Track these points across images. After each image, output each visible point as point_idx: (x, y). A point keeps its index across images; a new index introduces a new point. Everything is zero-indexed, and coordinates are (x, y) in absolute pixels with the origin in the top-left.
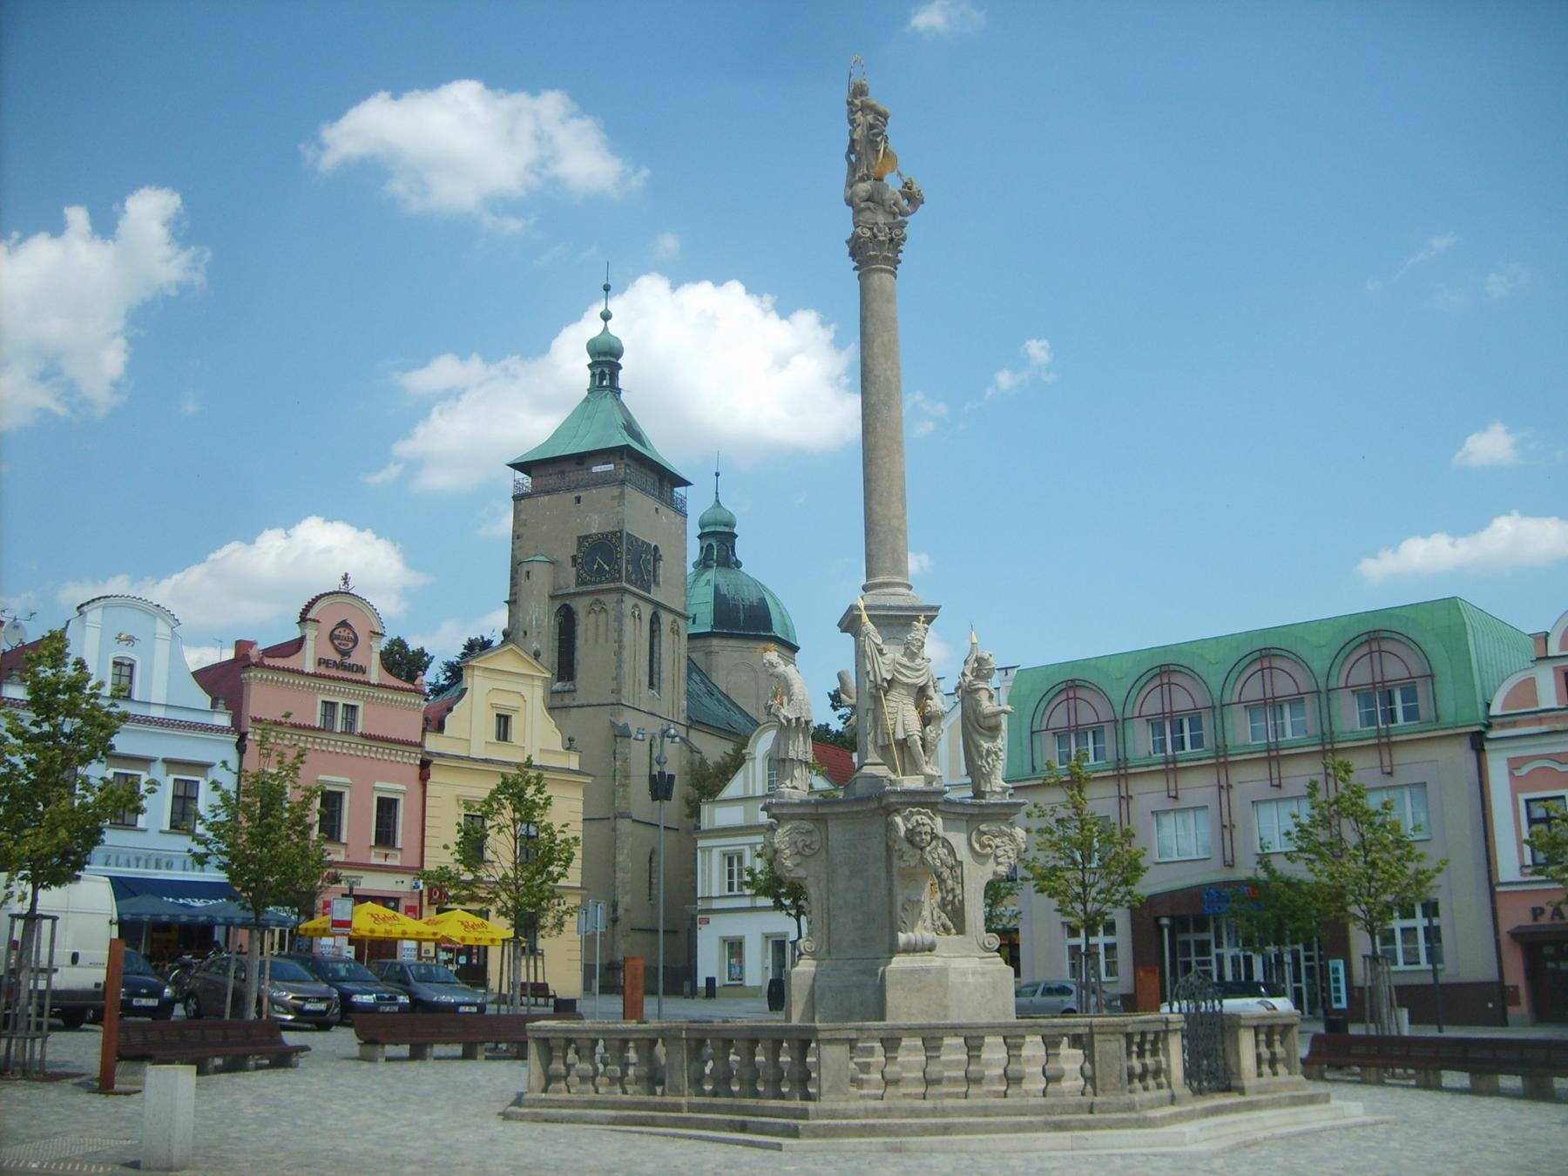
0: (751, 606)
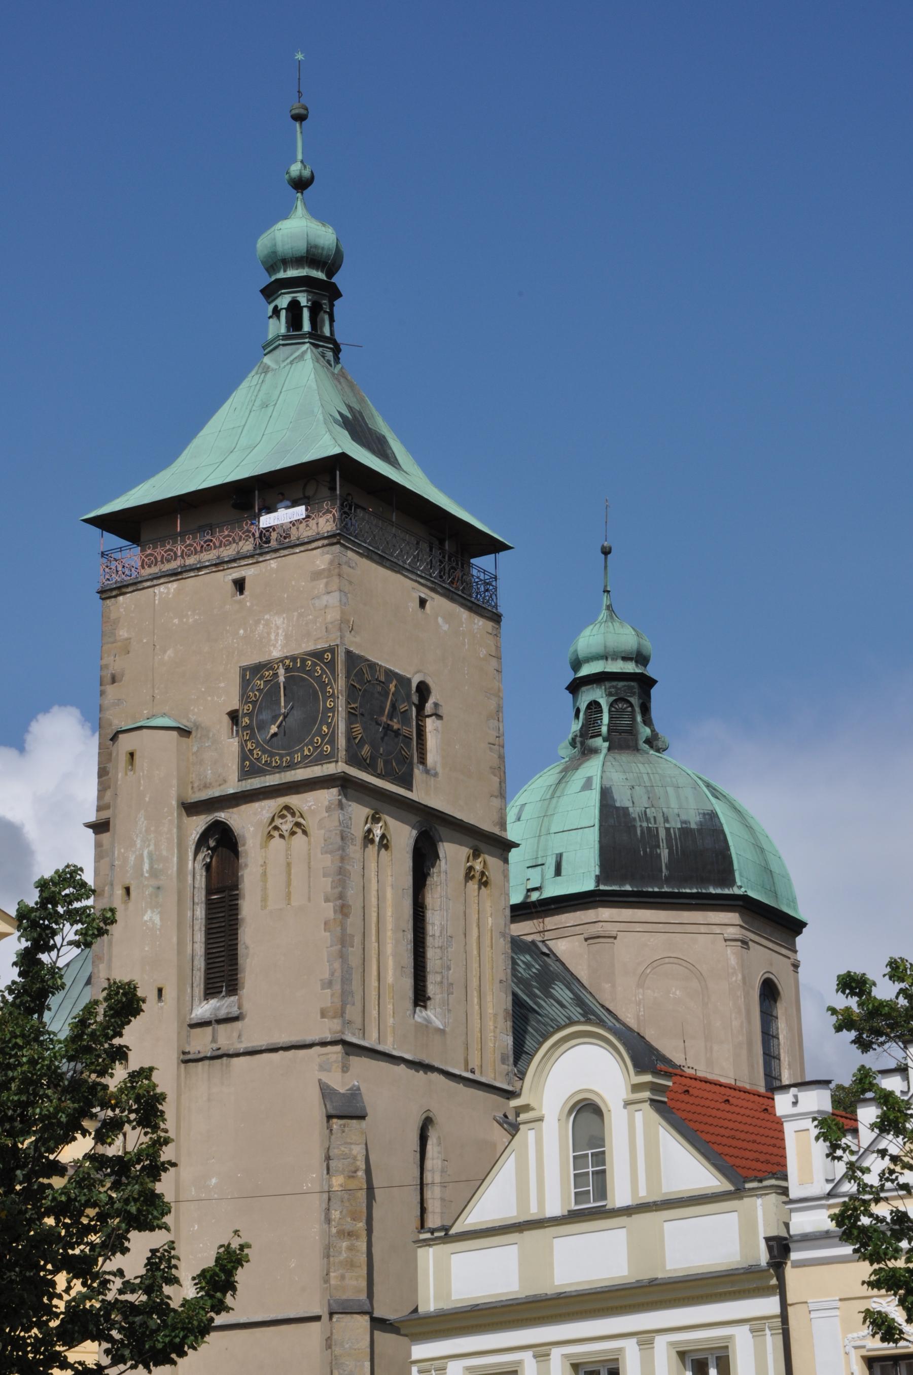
0: (685, 832)
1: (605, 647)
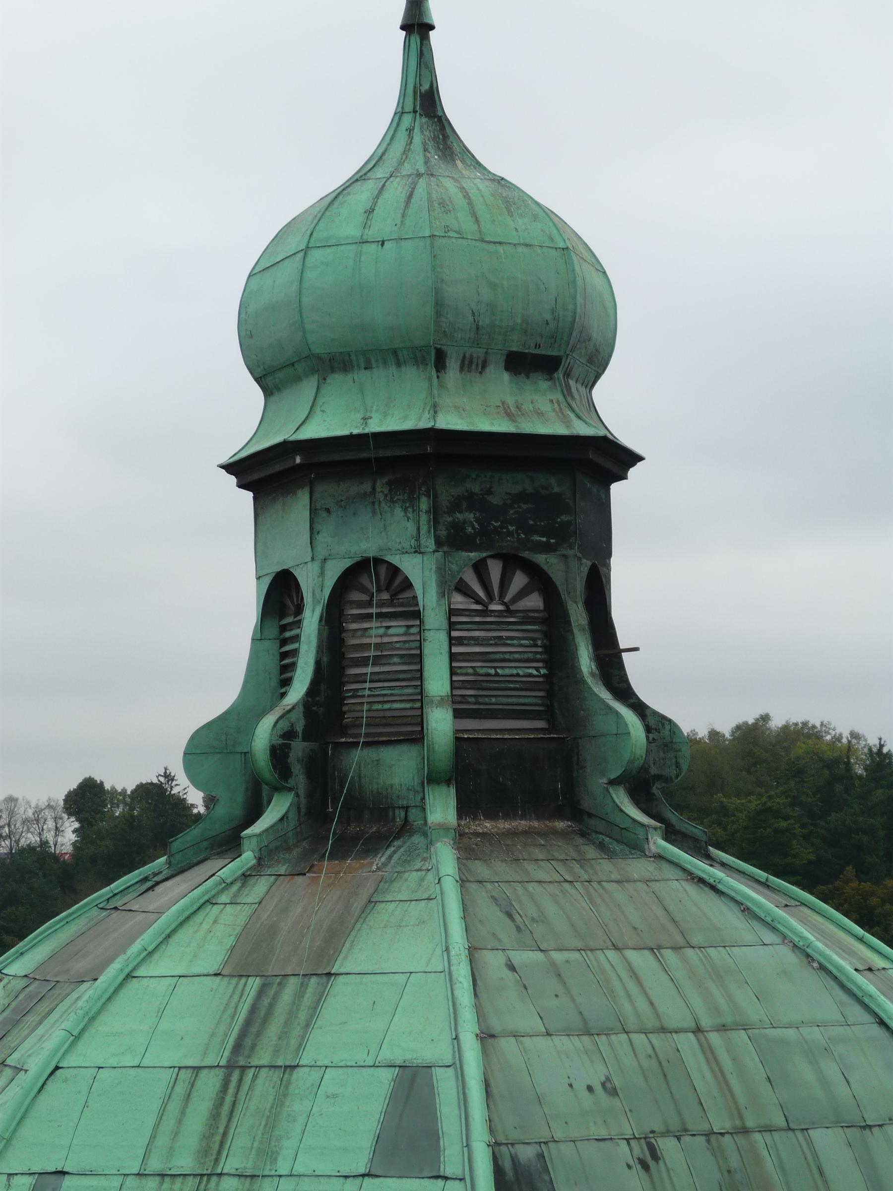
1: (439, 305)
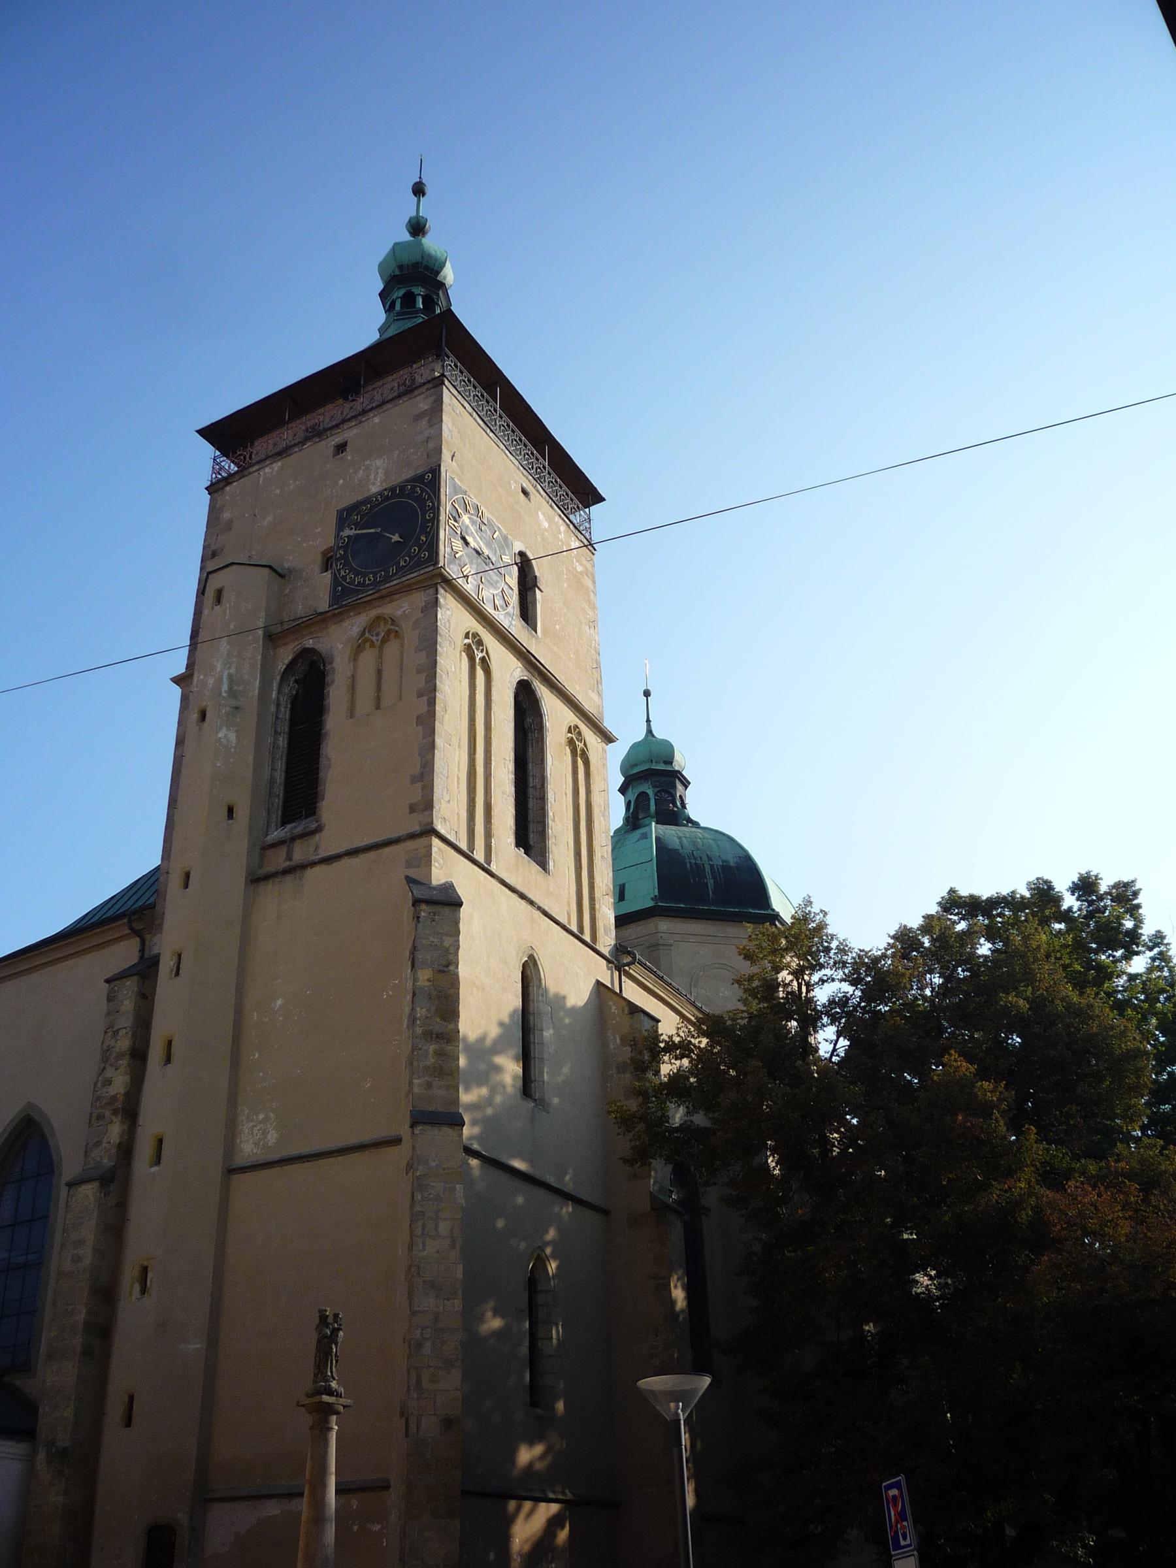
0: (726, 867)
